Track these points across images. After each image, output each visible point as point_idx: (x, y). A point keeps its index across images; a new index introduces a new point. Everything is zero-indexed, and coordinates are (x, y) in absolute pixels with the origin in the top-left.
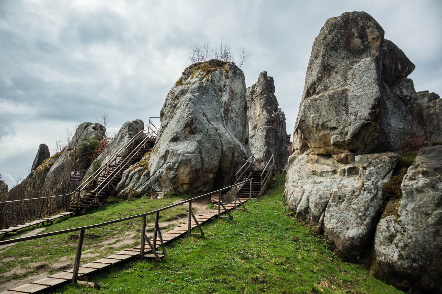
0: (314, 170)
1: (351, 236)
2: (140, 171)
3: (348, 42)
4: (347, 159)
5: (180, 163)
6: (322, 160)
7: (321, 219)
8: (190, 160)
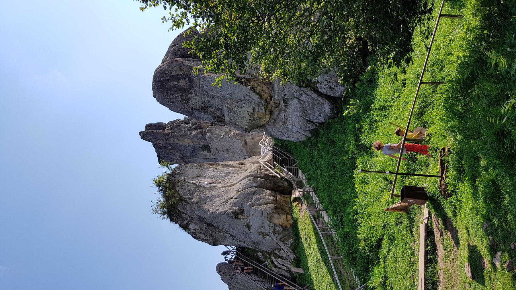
2: (275, 257)
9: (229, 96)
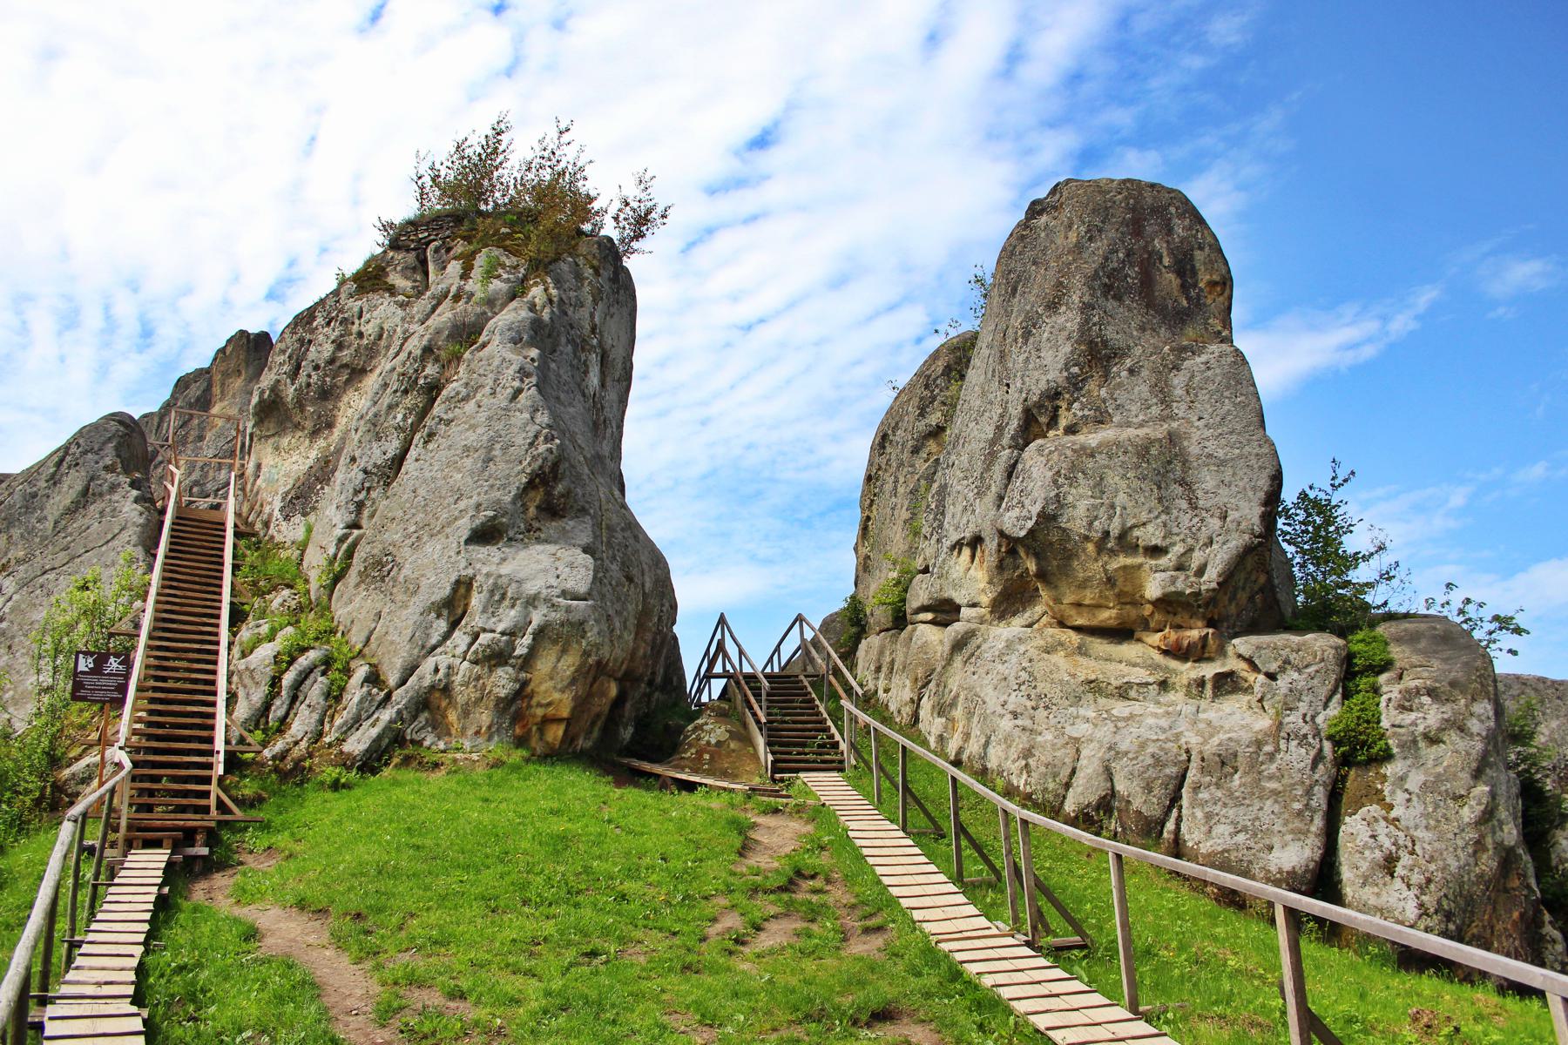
0: (1093, 677)
1: (1287, 867)
4: (1204, 647)
5: (540, 634)
6: (1100, 646)
7: (1170, 825)
8: (581, 623)
9: (1194, 450)
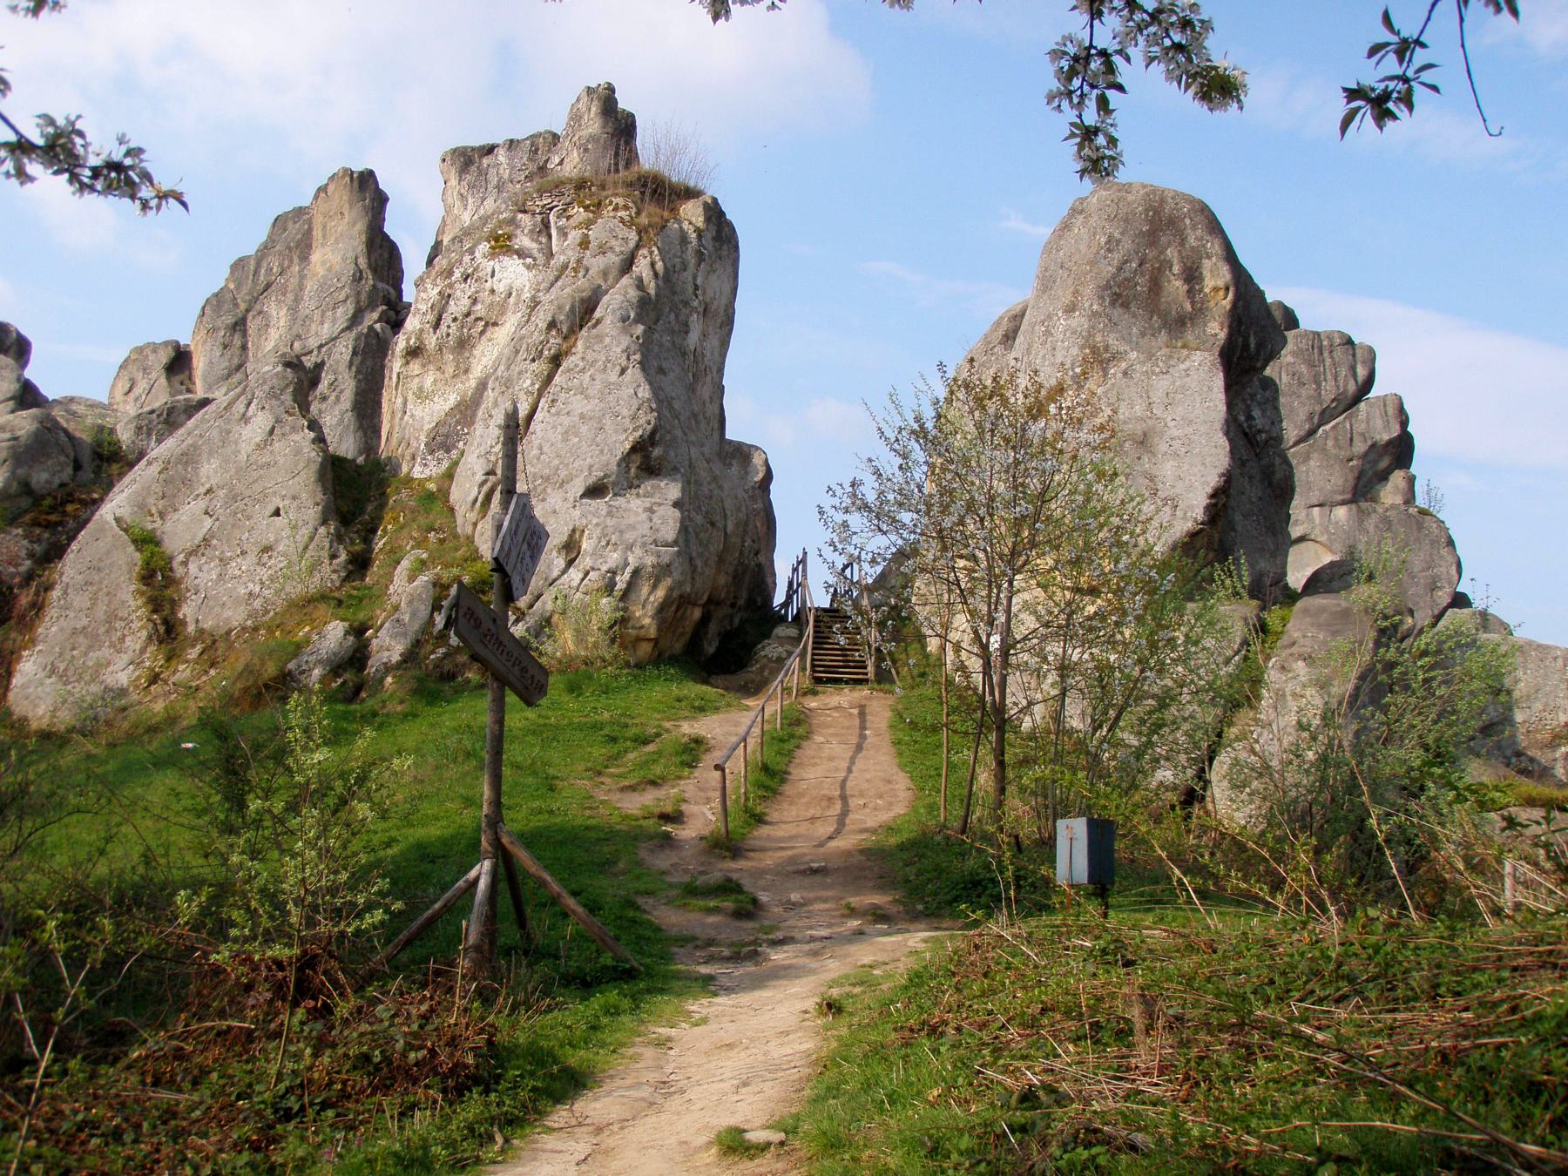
3: (1156, 286)
